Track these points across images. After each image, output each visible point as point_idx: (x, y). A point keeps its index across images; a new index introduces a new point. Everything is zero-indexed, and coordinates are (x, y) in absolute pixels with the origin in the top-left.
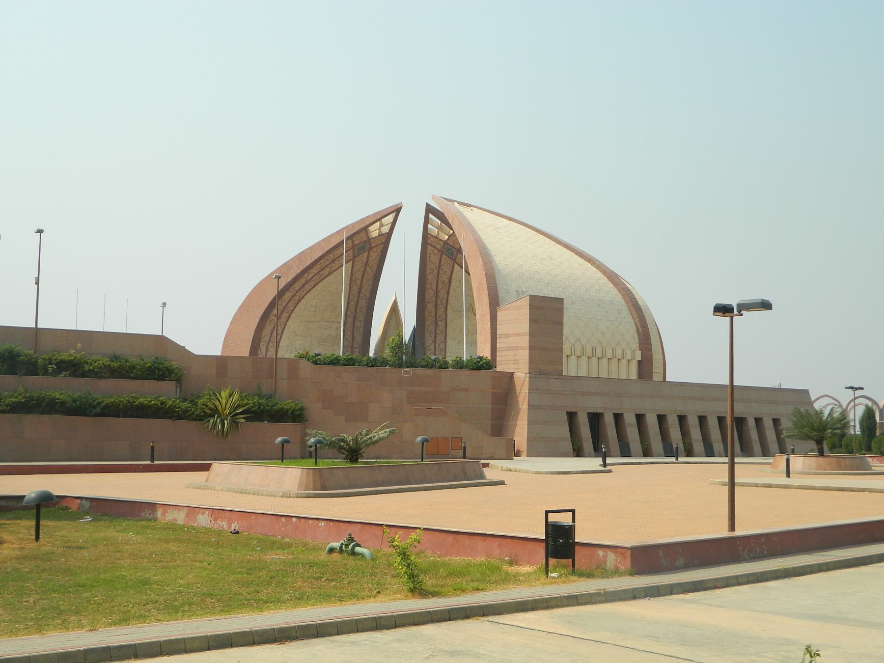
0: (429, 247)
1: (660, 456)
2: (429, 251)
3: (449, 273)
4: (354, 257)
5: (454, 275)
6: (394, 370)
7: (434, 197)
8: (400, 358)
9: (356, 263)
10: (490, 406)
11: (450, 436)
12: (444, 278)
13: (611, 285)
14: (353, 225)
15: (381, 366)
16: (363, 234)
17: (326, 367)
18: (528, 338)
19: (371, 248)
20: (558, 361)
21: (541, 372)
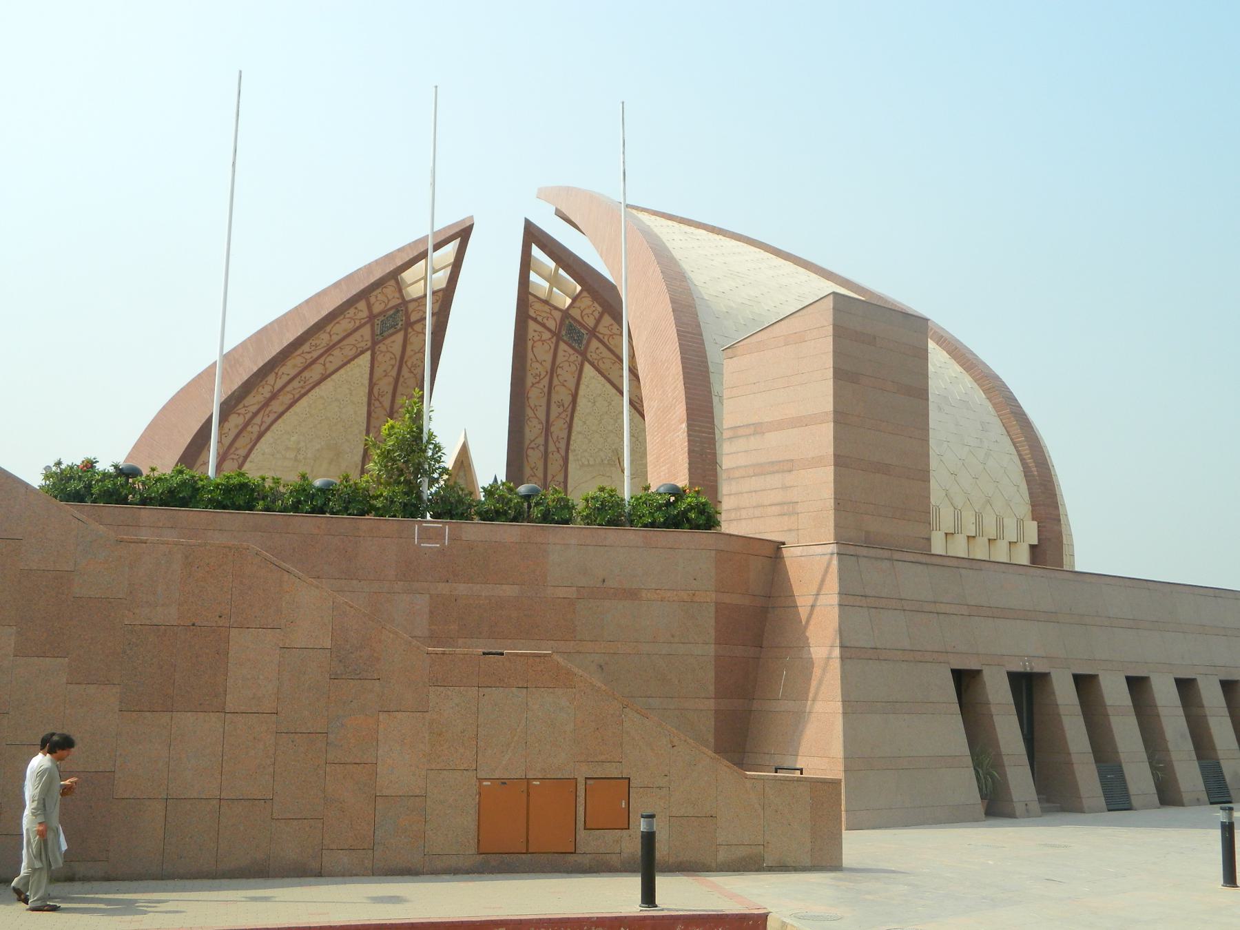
0: (532, 325)
1: (1198, 802)
2: (531, 334)
4: (375, 343)
6: (390, 525)
7: (544, 194)
8: (413, 488)
9: (380, 358)
10: (711, 649)
12: (562, 395)
13: (959, 369)
14: (369, 268)
15: (346, 510)
16: (390, 290)
17: (147, 513)
18: (832, 425)
19: (409, 324)
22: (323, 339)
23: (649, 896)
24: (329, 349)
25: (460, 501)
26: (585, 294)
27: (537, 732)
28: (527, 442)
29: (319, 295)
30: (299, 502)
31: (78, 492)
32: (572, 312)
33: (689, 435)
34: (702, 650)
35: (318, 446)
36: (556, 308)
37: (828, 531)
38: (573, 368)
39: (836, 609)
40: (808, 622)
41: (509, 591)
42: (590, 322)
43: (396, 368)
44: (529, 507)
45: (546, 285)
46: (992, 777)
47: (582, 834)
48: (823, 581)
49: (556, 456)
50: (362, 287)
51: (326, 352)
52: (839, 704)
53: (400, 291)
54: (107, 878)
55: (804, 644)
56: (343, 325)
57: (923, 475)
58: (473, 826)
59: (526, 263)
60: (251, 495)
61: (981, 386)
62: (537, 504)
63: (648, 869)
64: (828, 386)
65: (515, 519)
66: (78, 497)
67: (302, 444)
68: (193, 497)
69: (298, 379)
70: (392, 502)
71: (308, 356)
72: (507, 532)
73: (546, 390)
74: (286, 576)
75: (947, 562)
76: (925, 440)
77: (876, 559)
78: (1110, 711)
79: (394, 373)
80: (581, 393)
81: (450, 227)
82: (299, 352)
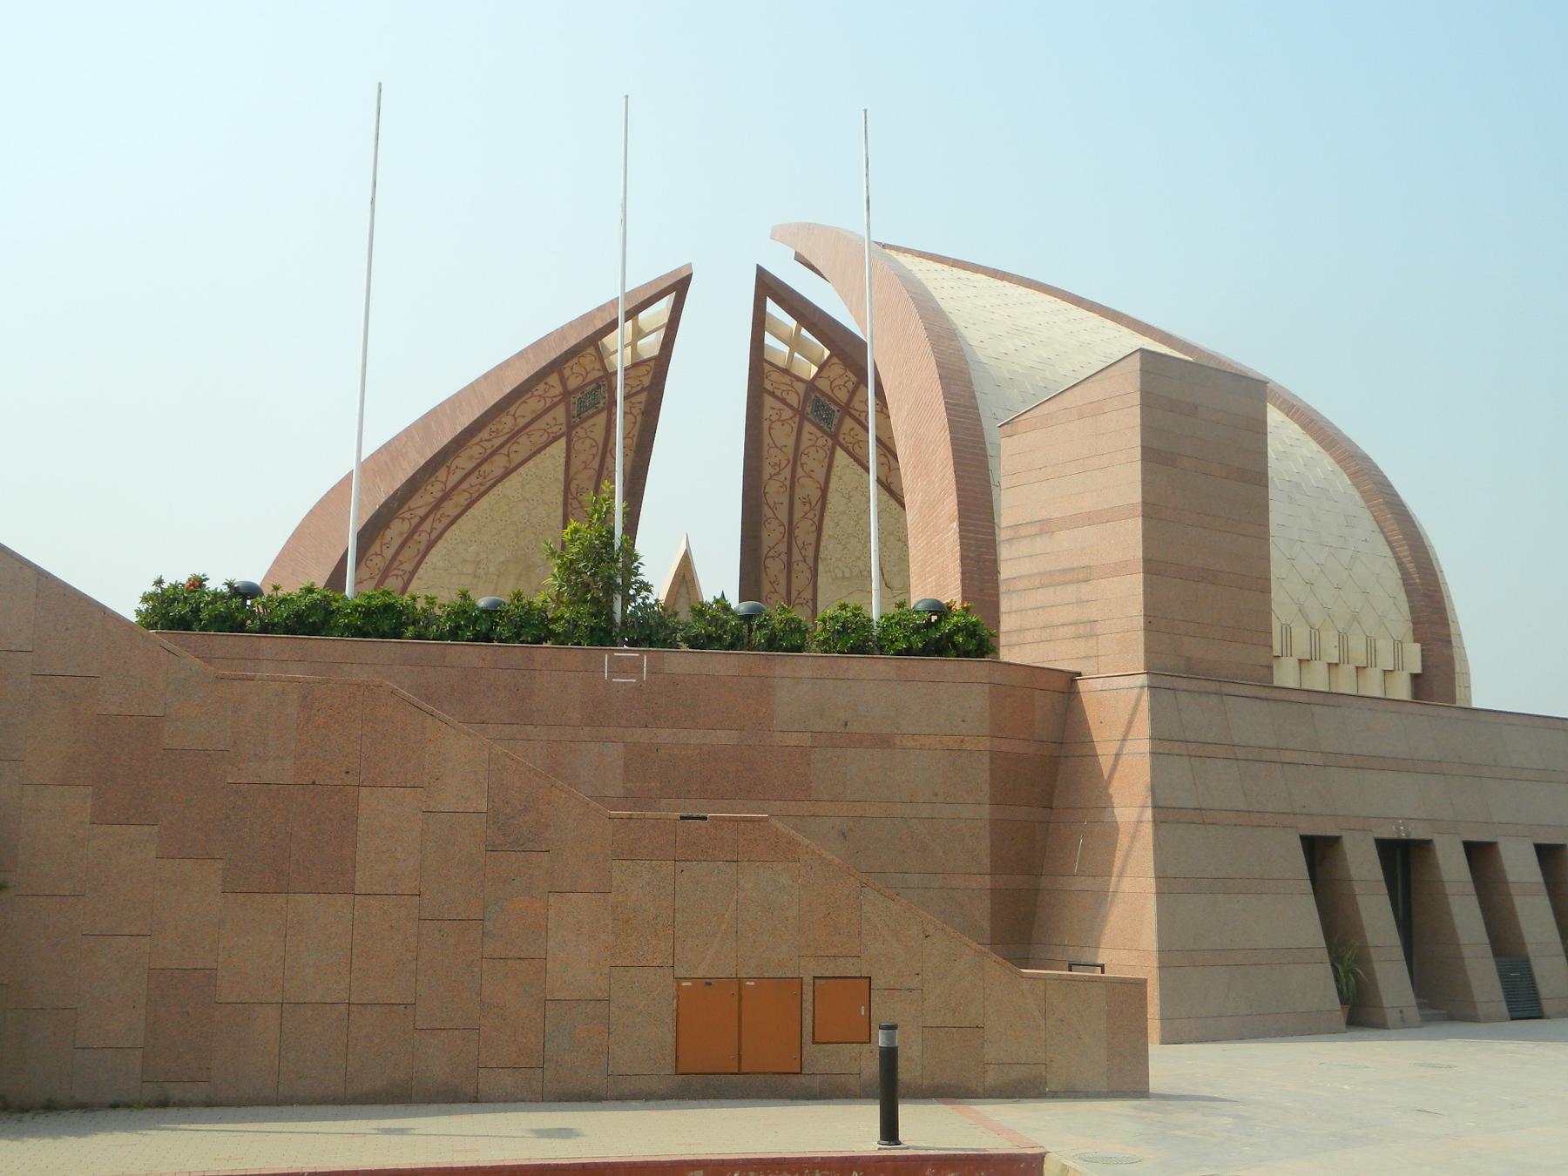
0: (769, 401)
3: (820, 474)
4: (571, 427)
5: (834, 479)
6: (573, 655)
8: (602, 608)
9: (577, 446)
10: (985, 811)
11: (810, 969)
12: (808, 488)
13: (1314, 446)
14: (561, 333)
15: (516, 637)
16: (588, 359)
18: (1140, 520)
20: (1253, 625)
21: (1192, 671)
22: (506, 423)
23: (890, 1131)
24: (514, 436)
25: (662, 624)
26: (835, 360)
27: (753, 919)
28: (765, 550)
29: (500, 367)
30: (459, 627)
31: (182, 618)
32: (821, 384)
33: (961, 537)
34: (975, 812)
35: (502, 558)
36: (799, 379)
37: (1136, 658)
38: (822, 454)
39: (1147, 758)
40: (1111, 775)
41: (723, 737)
42: (843, 396)
43: (598, 459)
44: (750, 630)
45: (786, 349)
46: (1356, 975)
47: (809, 1048)
48: (1130, 722)
49: (803, 566)
50: (553, 356)
51: (511, 438)
52: (1152, 882)
53: (601, 360)
54: (209, 1104)
55: (1106, 804)
56: (532, 405)
57: (1262, 586)
58: (670, 1039)
59: (760, 322)
60: (399, 618)
61: (1345, 469)
62: (760, 626)
63: (888, 1097)
64: (1132, 472)
65: (731, 647)
66: (183, 624)
67: (483, 556)
68: (325, 622)
69: (476, 474)
70: (576, 626)
71: (487, 445)
72: (719, 663)
73: (788, 483)
74: (429, 720)
75: (1293, 697)
76: (1263, 537)
77: (1200, 693)
78: (1513, 889)
79: (595, 464)
80: (832, 486)
81: (661, 278)
82: (477, 439)
